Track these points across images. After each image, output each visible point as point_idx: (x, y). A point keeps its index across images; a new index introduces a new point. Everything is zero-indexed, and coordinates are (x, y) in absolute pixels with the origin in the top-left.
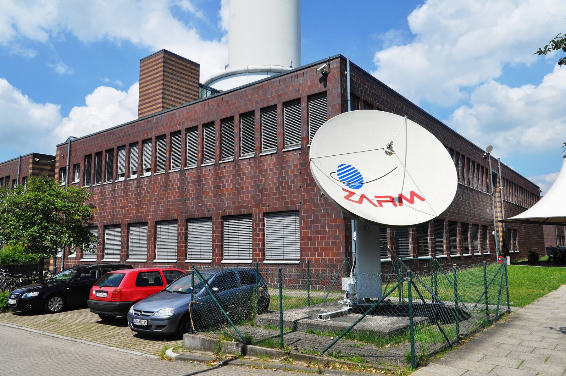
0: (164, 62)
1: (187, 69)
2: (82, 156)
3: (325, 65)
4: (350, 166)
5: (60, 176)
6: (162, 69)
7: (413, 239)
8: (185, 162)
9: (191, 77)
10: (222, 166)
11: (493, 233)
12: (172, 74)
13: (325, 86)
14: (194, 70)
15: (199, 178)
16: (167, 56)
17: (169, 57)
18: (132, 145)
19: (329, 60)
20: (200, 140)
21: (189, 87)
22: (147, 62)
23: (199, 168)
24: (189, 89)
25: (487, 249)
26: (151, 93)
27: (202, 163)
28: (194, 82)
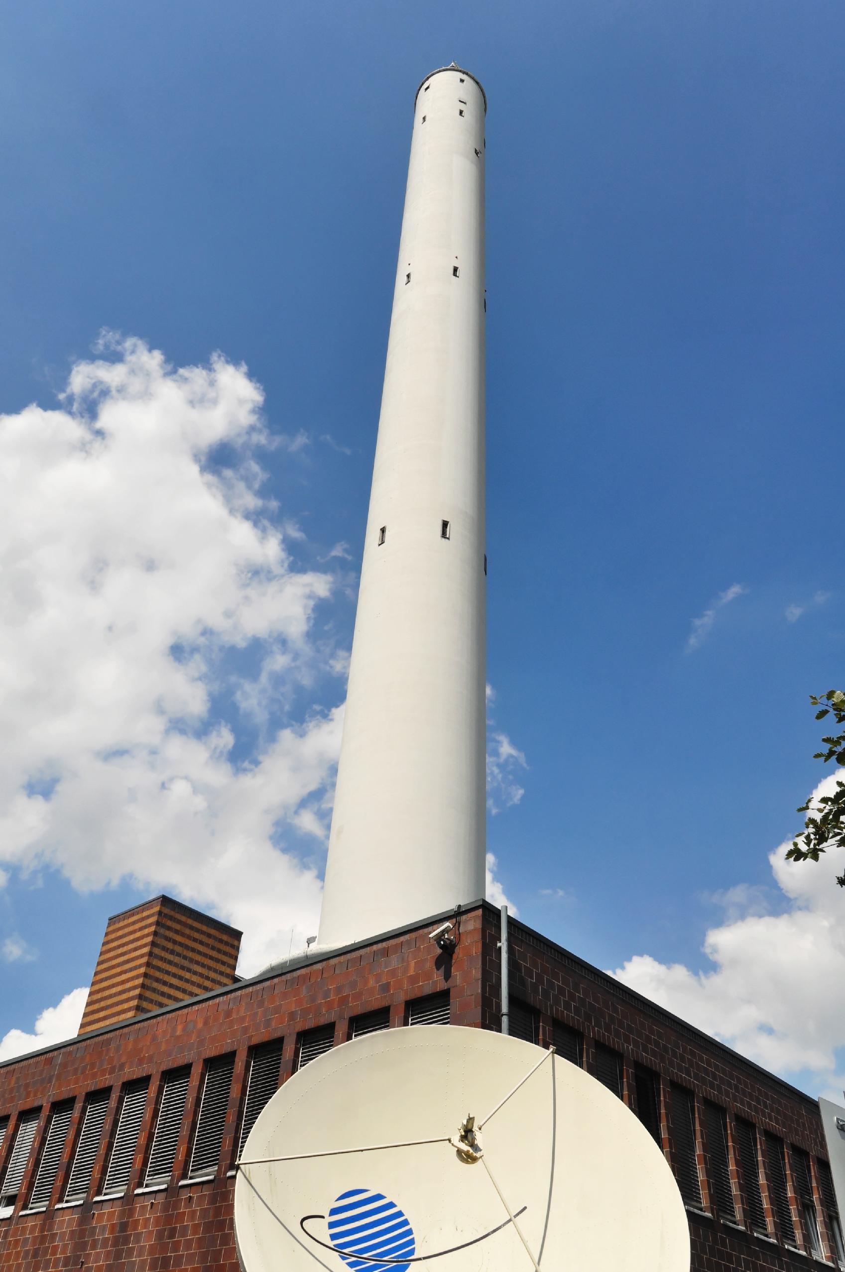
0: (158, 923)
3: (447, 924)
4: (379, 1197)
6: (149, 939)
8: (102, 1180)
10: (185, 1195)
12: (172, 952)
13: (447, 976)
14: (227, 944)
15: (124, 1231)
16: (166, 911)
17: (172, 913)
19: (457, 914)
20: (148, 1116)
22: (121, 924)
23: (129, 1199)
26: (115, 995)
27: (140, 1185)
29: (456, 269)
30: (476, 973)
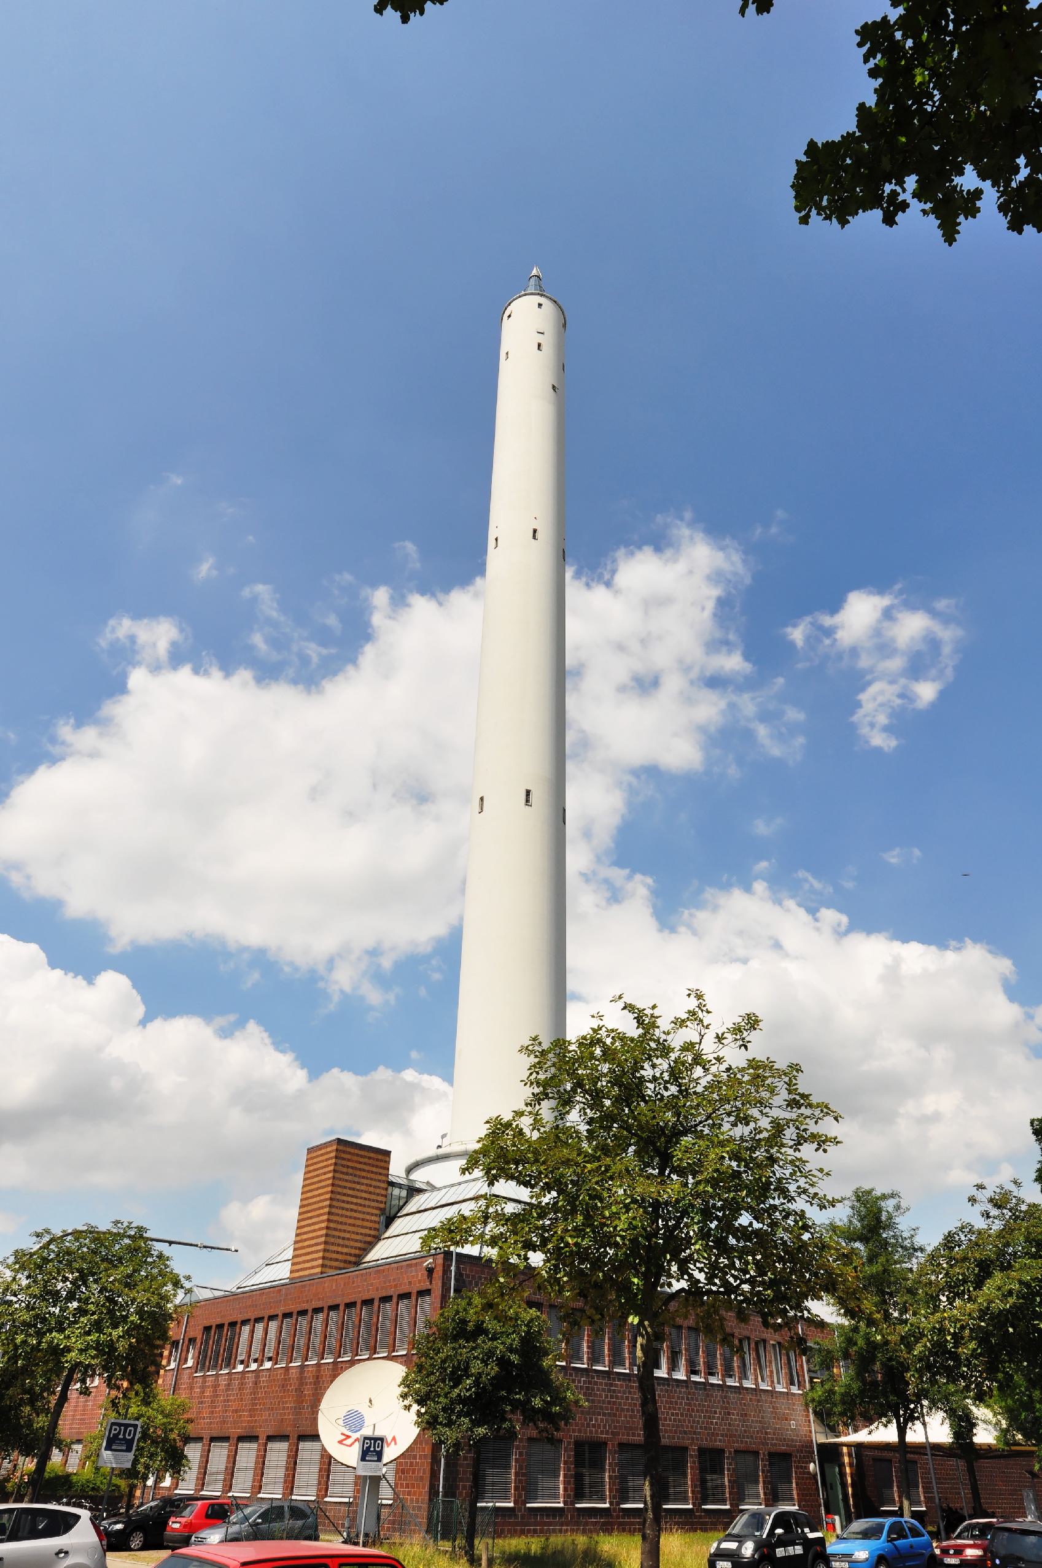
0: (336, 1157)
1: (371, 1161)
2: (201, 1327)
5: (171, 1353)
6: (332, 1168)
7: (565, 1476)
9: (376, 1173)
10: (340, 1365)
11: (812, 1465)
12: (347, 1174)
14: (381, 1161)
16: (341, 1148)
18: (258, 1320)
21: (372, 1189)
24: (370, 1193)
25: (792, 1499)
28: (379, 1181)
29: (535, 531)
30: (440, 1284)
